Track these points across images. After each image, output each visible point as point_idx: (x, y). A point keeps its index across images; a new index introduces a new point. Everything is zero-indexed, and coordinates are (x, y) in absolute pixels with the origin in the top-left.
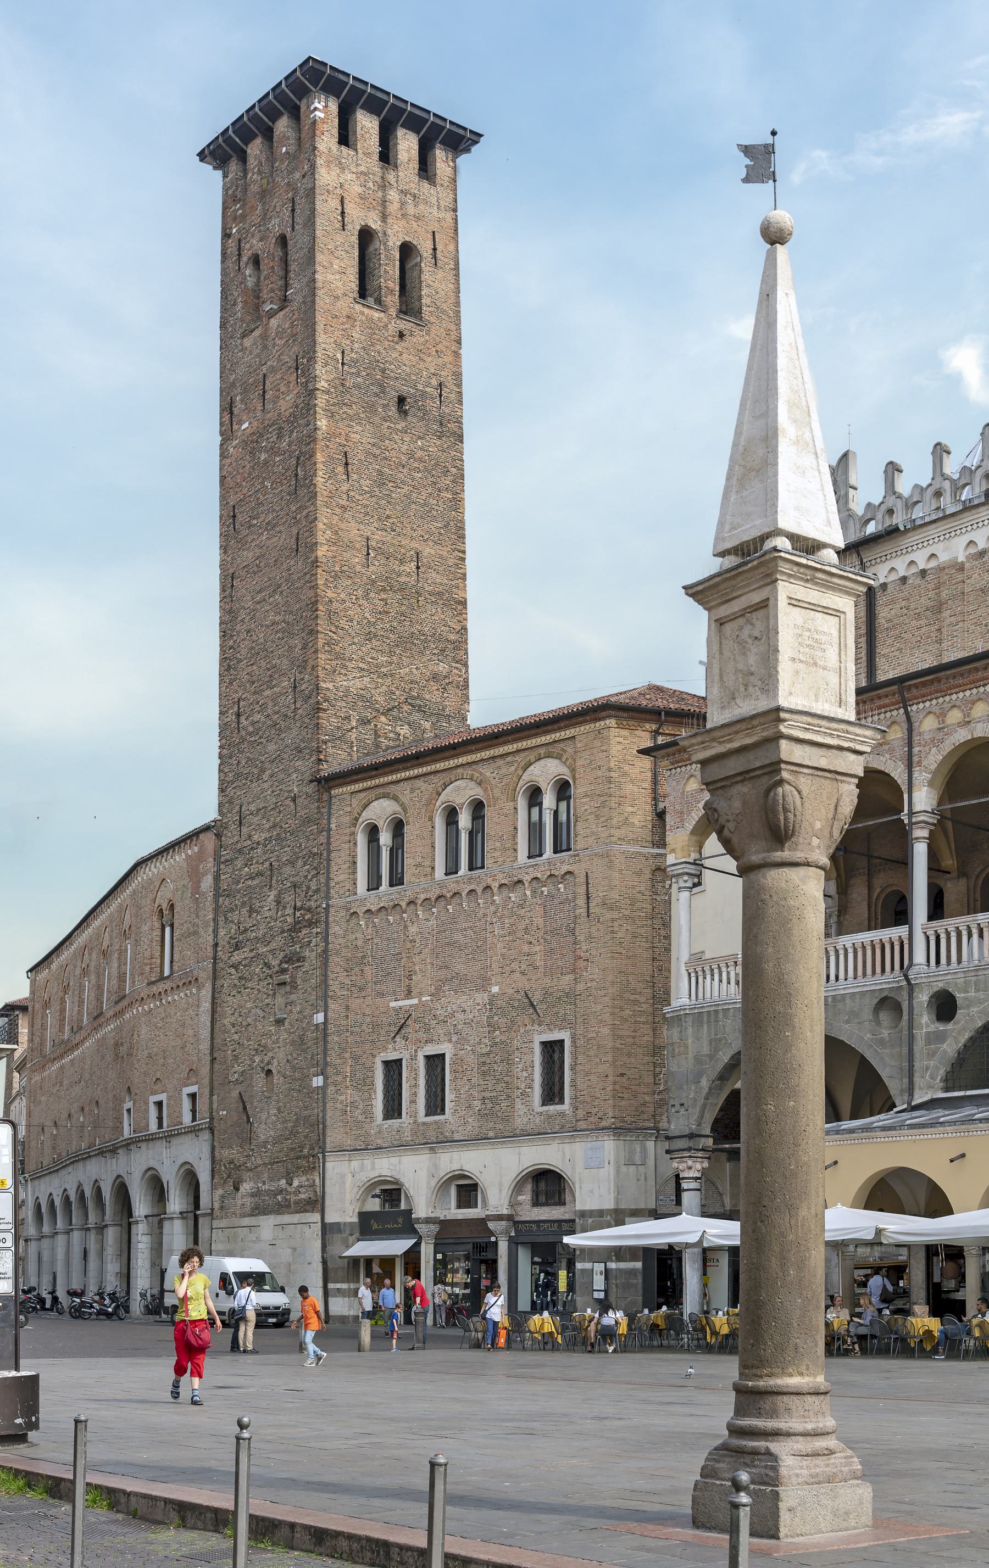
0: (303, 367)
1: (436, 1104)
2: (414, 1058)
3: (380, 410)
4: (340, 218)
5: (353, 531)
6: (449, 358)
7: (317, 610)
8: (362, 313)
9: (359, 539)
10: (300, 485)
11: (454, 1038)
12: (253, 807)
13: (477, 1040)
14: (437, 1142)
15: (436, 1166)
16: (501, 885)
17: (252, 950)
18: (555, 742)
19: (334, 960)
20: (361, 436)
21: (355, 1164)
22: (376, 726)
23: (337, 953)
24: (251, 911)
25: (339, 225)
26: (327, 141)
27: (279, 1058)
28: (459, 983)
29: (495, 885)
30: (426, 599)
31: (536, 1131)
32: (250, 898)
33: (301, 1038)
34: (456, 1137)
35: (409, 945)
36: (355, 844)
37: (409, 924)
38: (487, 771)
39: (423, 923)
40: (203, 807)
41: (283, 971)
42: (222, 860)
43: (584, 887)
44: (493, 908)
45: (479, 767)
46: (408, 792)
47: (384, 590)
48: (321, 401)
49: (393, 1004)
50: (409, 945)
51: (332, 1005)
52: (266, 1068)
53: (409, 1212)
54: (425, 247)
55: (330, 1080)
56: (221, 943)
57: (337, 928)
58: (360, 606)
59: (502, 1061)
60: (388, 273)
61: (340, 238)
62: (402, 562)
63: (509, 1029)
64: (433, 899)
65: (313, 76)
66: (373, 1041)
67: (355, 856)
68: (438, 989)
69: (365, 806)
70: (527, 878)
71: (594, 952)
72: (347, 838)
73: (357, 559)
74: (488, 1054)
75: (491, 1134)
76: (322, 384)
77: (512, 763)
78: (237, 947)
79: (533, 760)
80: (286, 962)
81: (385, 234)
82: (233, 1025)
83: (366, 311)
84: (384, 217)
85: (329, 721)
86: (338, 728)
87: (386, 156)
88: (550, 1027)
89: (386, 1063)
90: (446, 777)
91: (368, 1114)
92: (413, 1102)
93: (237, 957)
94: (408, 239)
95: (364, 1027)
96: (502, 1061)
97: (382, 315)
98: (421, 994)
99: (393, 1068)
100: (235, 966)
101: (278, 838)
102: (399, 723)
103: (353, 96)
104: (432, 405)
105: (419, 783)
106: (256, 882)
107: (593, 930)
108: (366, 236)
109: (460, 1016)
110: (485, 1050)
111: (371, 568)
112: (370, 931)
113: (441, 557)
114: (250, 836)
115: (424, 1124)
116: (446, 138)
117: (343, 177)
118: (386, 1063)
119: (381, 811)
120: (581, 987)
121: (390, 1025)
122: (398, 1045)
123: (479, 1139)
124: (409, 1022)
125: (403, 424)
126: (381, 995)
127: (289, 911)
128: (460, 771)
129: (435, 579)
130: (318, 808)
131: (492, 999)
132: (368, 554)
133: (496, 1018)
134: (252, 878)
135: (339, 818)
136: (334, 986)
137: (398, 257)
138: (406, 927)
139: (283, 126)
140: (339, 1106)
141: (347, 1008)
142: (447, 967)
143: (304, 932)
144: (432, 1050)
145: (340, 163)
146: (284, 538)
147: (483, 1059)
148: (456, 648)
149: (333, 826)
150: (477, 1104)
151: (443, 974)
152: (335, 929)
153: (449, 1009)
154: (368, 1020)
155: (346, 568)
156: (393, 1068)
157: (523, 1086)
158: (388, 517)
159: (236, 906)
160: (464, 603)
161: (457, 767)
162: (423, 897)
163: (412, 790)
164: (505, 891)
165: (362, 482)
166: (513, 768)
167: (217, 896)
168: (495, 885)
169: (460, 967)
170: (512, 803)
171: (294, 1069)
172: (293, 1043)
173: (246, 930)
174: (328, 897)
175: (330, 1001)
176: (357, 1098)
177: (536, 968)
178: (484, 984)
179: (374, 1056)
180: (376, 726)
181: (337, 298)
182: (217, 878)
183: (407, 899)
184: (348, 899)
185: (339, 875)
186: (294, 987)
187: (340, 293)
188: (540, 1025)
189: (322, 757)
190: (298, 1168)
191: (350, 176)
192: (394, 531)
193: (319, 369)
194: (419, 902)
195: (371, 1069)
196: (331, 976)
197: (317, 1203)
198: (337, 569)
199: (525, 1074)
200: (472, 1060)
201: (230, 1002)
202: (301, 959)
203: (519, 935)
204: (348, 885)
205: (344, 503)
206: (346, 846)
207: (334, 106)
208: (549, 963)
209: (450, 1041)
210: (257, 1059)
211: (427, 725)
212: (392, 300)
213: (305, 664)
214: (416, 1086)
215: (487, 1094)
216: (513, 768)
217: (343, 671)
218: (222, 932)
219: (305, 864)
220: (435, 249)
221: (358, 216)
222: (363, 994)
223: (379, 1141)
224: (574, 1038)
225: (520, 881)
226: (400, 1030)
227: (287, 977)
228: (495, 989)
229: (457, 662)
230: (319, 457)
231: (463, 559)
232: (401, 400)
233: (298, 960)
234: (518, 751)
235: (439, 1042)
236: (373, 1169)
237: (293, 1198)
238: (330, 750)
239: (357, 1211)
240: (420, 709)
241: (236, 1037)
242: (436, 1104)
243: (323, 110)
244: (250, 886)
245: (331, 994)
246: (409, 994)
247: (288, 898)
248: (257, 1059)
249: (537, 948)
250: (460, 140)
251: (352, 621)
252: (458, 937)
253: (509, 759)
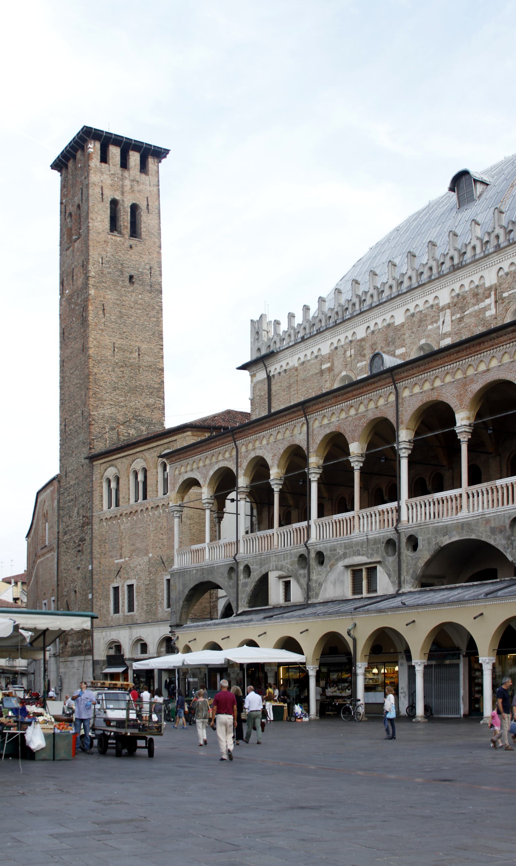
0: (85, 266)
1: (131, 608)
2: (123, 586)
3: (120, 283)
4: (101, 196)
5: (107, 341)
6: (155, 255)
7: (89, 378)
8: (112, 239)
9: (110, 344)
10: (84, 322)
11: (137, 578)
12: (70, 469)
14: (131, 624)
15: (131, 635)
16: (152, 507)
18: (170, 442)
19: (95, 541)
20: (111, 296)
21: (104, 634)
22: (118, 430)
23: (96, 538)
24: (70, 517)
25: (100, 200)
26: (95, 162)
27: (79, 584)
29: (150, 508)
30: (143, 369)
31: (165, 620)
32: (69, 511)
34: (138, 622)
36: (102, 487)
37: (121, 525)
38: (147, 454)
39: (125, 524)
40: (55, 470)
41: (79, 545)
44: (149, 518)
45: (144, 453)
46: (120, 464)
47: (122, 367)
48: (91, 281)
49: (116, 561)
51: (95, 562)
53: (123, 655)
54: (143, 205)
55: (94, 596)
56: (61, 531)
57: (96, 526)
58: (110, 375)
60: (125, 219)
61: (101, 205)
62: (131, 353)
63: (156, 573)
65: (88, 134)
67: (102, 493)
68: (131, 555)
69: (106, 470)
70: (160, 505)
71: (183, 539)
72: (99, 485)
73: (109, 353)
74: (148, 585)
75: (150, 621)
76: (92, 274)
81: (123, 201)
82: (64, 569)
83: (113, 238)
84: (123, 193)
85: (95, 430)
86: (100, 433)
87: (124, 164)
91: (108, 611)
92: (123, 606)
93: (65, 539)
94: (134, 202)
95: (106, 572)
97: (122, 238)
98: (125, 557)
99: (116, 589)
100: (64, 542)
101: (78, 484)
102: (130, 428)
103: (106, 140)
104: (147, 278)
105: (124, 460)
108: (114, 203)
109: (138, 567)
111: (116, 357)
112: (107, 527)
113: (151, 349)
114: (69, 482)
115: (127, 616)
116: (151, 154)
117: (103, 177)
119: (111, 472)
121: (115, 571)
123: (146, 623)
124: (121, 570)
125: (132, 288)
126: (112, 557)
127: (81, 518)
128: (138, 454)
129: (147, 359)
132: (114, 350)
134: (70, 502)
135: (96, 476)
137: (129, 211)
138: (120, 526)
139: (79, 154)
140: (97, 607)
141: (100, 563)
142: (134, 545)
143: (86, 527)
144: (129, 582)
145: (101, 171)
146: (79, 345)
147: (146, 587)
148: (158, 391)
150: (145, 607)
152: (95, 527)
154: (107, 568)
155: (103, 358)
156: (116, 589)
157: (160, 599)
158: (124, 332)
160: (162, 370)
162: (125, 512)
163: (122, 463)
165: (111, 317)
167: (59, 509)
168: (150, 508)
169: (138, 545)
170: (155, 470)
171: (83, 590)
172: (83, 578)
174: (92, 512)
175: (94, 560)
176: (104, 604)
177: (164, 546)
179: (110, 585)
180: (118, 430)
181: (99, 233)
182: (59, 502)
184: (100, 513)
185: (96, 502)
187: (100, 231)
189: (91, 447)
190: (85, 635)
191: (106, 177)
192: (127, 338)
193: (90, 267)
194: (124, 514)
195: (108, 591)
196: (94, 548)
197: (90, 652)
198: (99, 359)
200: (143, 587)
201: (63, 558)
202: (85, 540)
203: (158, 530)
204: (99, 507)
205: (102, 328)
206: (98, 488)
207: (98, 145)
208: (169, 543)
209: (135, 578)
210: (72, 585)
211: (144, 428)
212: (127, 231)
213: (85, 404)
215: (148, 603)
217: (102, 406)
218: (61, 526)
221: (109, 195)
222: (106, 556)
223: (112, 624)
225: (158, 506)
227: (80, 548)
228: (151, 555)
229: (159, 398)
230: (90, 308)
231: (162, 349)
232: (131, 277)
234: (157, 446)
235: (131, 579)
236: (110, 636)
237: (84, 649)
238: (96, 443)
239: (106, 655)
240: (140, 421)
241: (65, 575)
242: (131, 608)
243: (93, 148)
244: (69, 506)
245: (94, 556)
246: (121, 557)
247: (81, 512)
249: (165, 537)
250: (160, 154)
251: (106, 382)
252: (138, 531)
253: (155, 449)
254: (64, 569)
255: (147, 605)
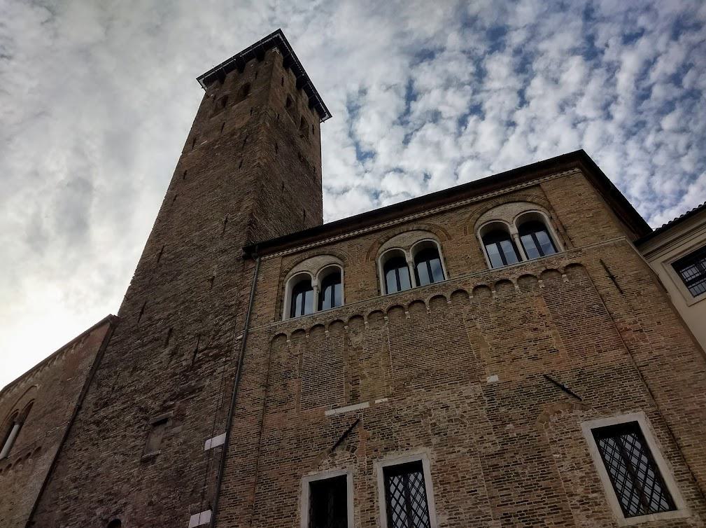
11: (435, 440)
13: (476, 438)
16: (476, 288)
17: (123, 403)
28: (433, 379)
29: (469, 289)
33: (180, 472)
35: (352, 353)
36: (283, 288)
42: (111, 342)
43: (603, 272)
44: (468, 308)
45: (428, 221)
50: (352, 353)
51: (238, 423)
52: (112, 519)
56: (85, 405)
59: (528, 460)
64: (385, 310)
66: (298, 459)
67: (282, 296)
69: (298, 263)
74: (500, 454)
77: (465, 213)
78: (106, 405)
79: (489, 206)
80: (171, 400)
88: (604, 410)
89: (318, 488)
90: (391, 233)
95: (284, 443)
96: (528, 460)
98: (373, 397)
106: (145, 348)
107: (635, 303)
110: (492, 450)
118: (318, 488)
120: (640, 358)
122: (338, 460)
124: (357, 429)
128: (404, 228)
130: (242, 275)
131: (490, 391)
133: (503, 410)
134: (143, 345)
136: (245, 404)
138: (347, 338)
144: (395, 459)
147: (494, 461)
149: (261, 279)
151: (405, 372)
153: (420, 407)
154: (291, 434)
157: (580, 490)
159: (116, 373)
161: (402, 224)
162: (370, 310)
163: (351, 246)
164: (484, 293)
166: (467, 216)
168: (469, 289)
173: (122, 387)
175: (236, 420)
178: (474, 375)
179: (297, 477)
183: (350, 315)
186: (181, 417)
188: (583, 410)
195: (293, 494)
196: (241, 393)
199: (578, 474)
200: (471, 465)
209: (428, 444)
210: (99, 512)
214: (372, 509)
215: (509, 509)
216: (467, 216)
218: (89, 397)
219: (216, 317)
220: (313, 129)
222: (285, 407)
224: (659, 419)
226: (342, 440)
228: (493, 379)
233: (193, 392)
234: (472, 204)
235: (408, 446)
241: (75, 492)
246: (355, 398)
248: (99, 512)
249: (550, 333)
254: (75, 480)
255: (506, 516)
